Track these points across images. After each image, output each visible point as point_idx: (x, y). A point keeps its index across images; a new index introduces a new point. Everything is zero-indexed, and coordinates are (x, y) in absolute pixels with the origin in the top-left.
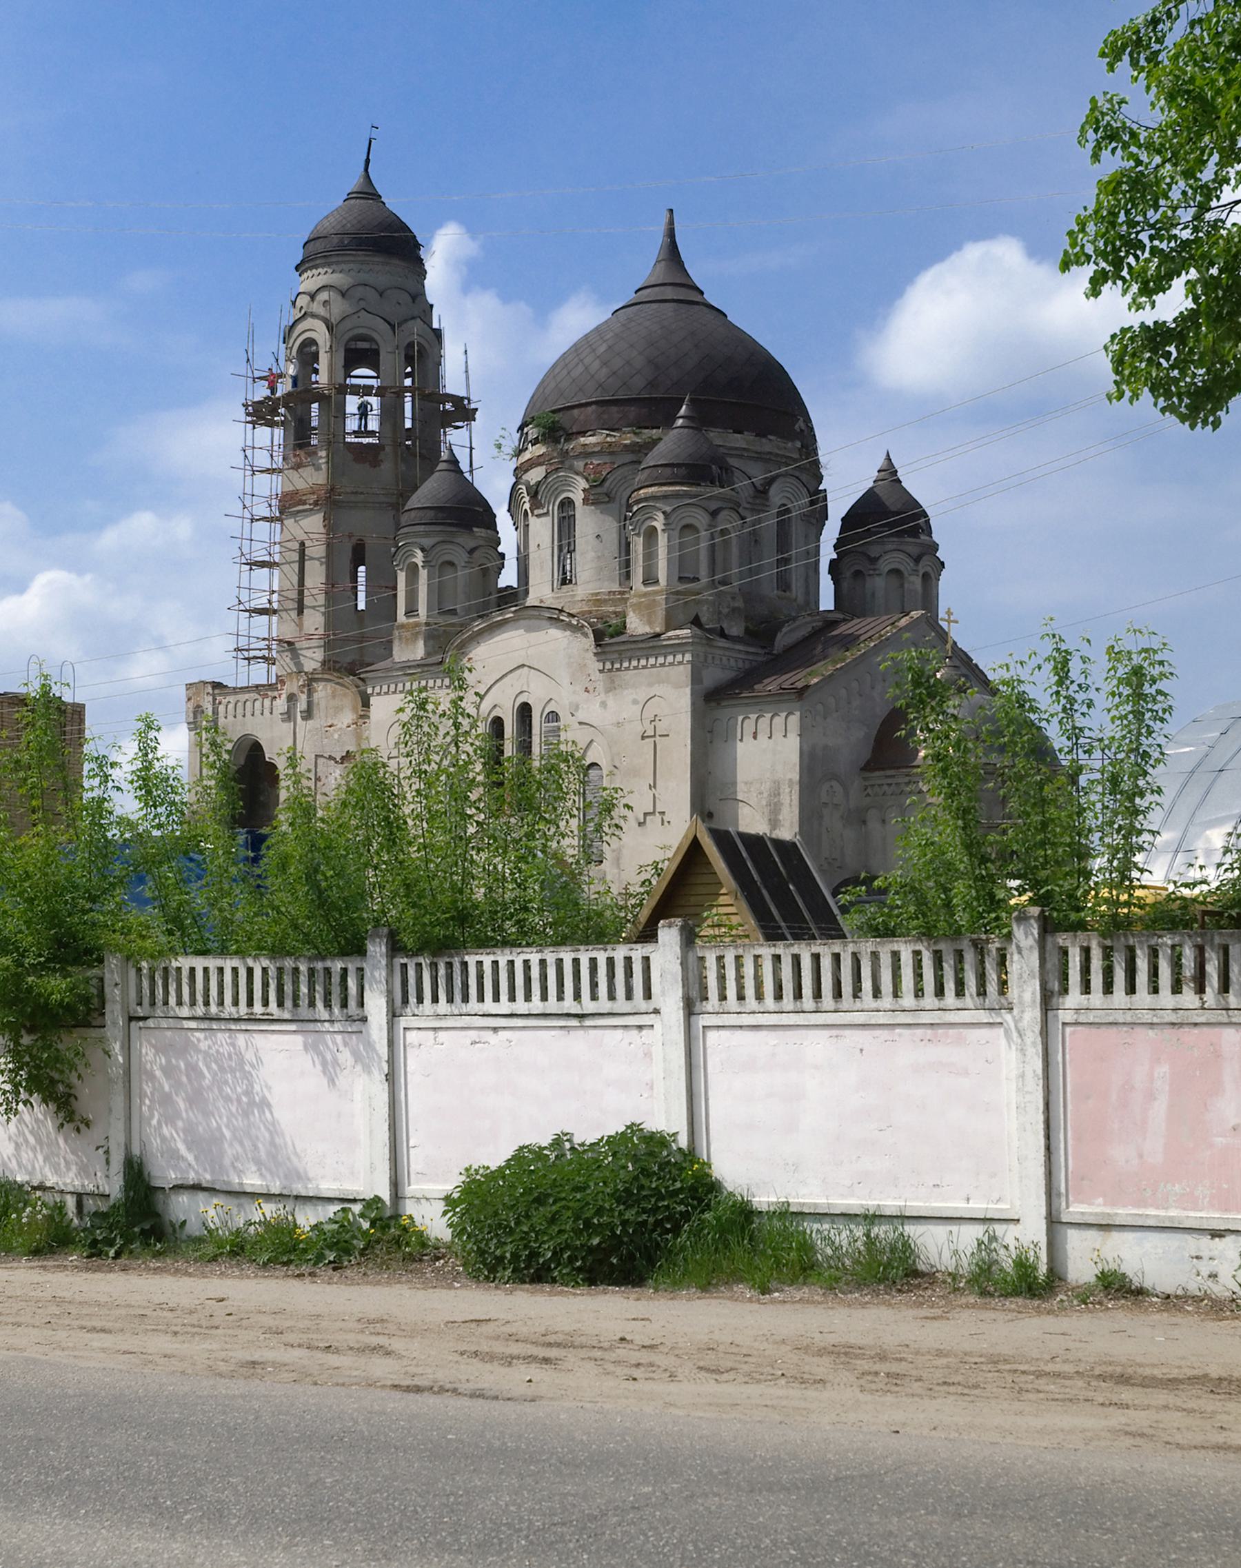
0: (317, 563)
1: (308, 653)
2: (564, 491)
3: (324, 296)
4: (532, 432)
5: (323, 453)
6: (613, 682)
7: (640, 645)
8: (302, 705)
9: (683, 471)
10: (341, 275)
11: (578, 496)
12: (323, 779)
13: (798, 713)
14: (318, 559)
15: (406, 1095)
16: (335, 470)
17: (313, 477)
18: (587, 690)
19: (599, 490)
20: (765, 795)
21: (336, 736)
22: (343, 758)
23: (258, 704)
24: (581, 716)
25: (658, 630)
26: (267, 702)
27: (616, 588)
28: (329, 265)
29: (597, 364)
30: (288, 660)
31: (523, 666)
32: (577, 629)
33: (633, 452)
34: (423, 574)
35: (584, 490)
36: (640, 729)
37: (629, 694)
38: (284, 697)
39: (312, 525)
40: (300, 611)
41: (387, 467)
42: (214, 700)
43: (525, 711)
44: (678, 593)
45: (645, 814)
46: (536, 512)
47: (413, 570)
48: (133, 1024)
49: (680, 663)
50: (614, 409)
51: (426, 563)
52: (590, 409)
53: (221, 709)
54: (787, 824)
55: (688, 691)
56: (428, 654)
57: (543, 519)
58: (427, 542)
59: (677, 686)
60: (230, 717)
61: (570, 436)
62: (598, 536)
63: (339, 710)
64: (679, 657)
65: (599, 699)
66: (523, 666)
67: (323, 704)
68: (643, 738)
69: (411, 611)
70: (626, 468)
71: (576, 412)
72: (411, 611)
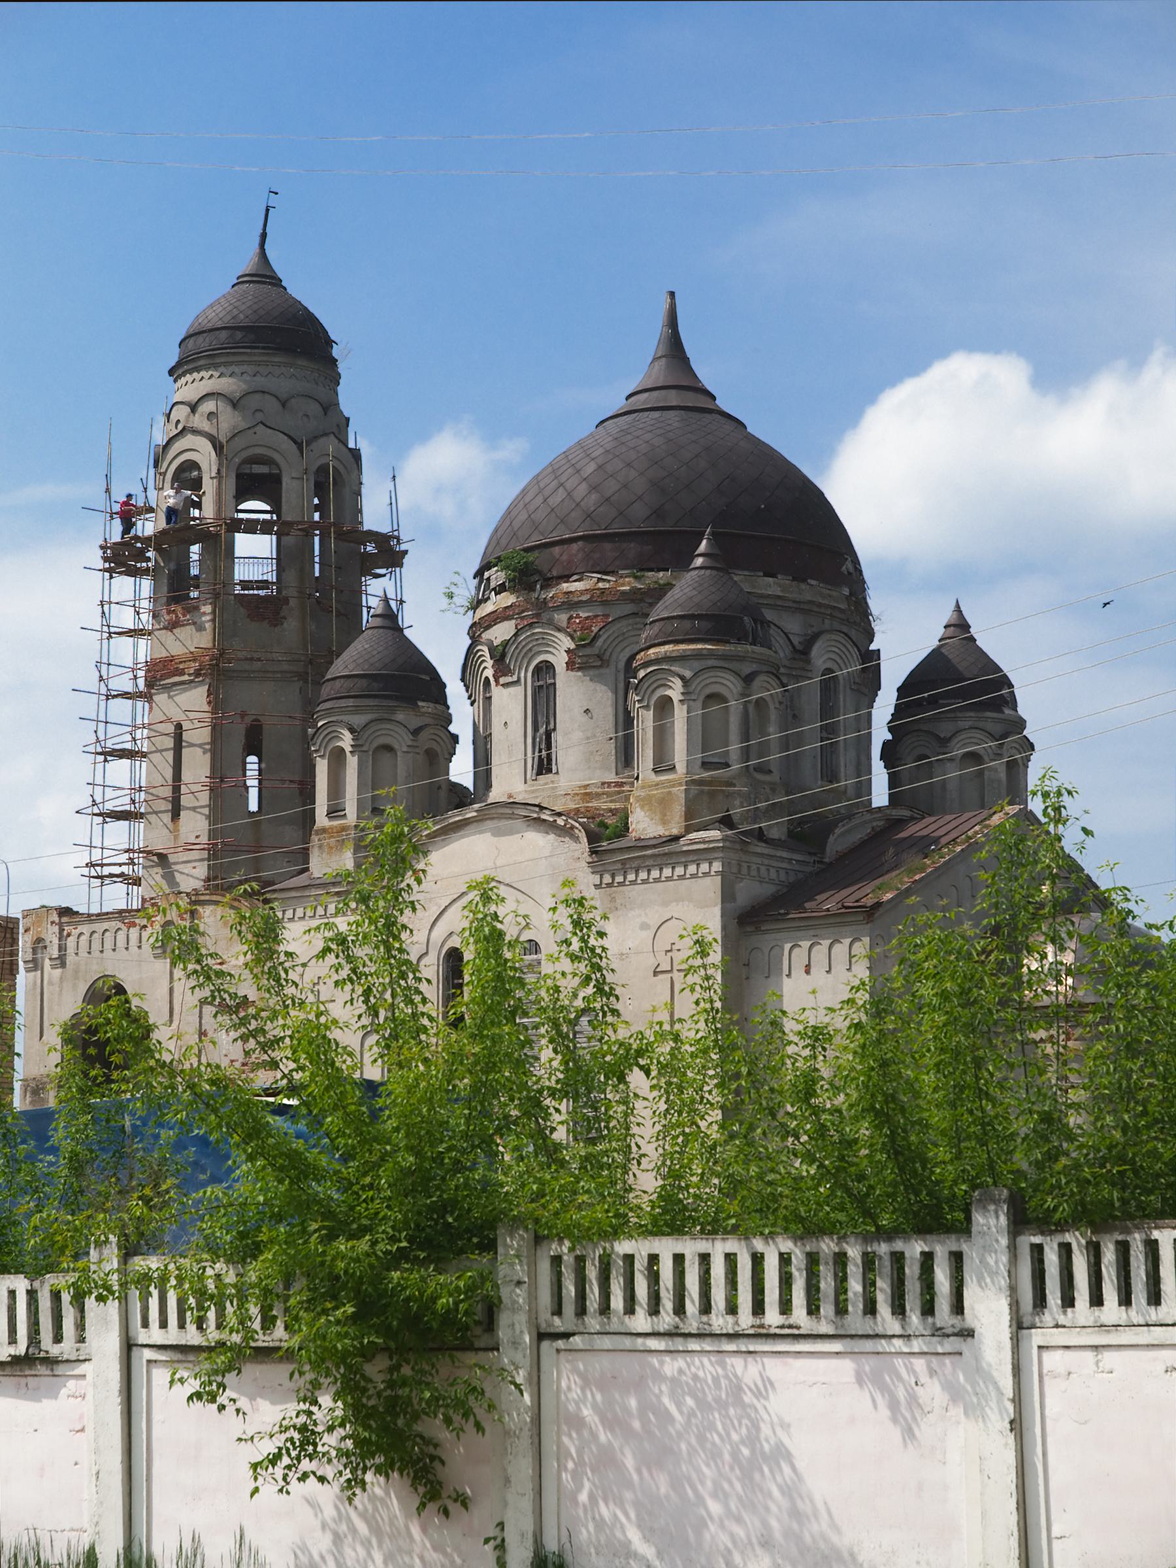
0: (199, 751)
1: (187, 868)
2: (540, 652)
3: (209, 406)
4: (497, 576)
5: (208, 609)
6: (613, 900)
9: (706, 625)
10: (230, 380)
11: (559, 659)
13: (866, 940)
14: (200, 746)
15: (1044, 1454)
16: (223, 631)
17: (193, 640)
19: (588, 651)
23: (121, 936)
25: (675, 831)
26: (134, 933)
27: (612, 777)
28: (215, 366)
29: (583, 488)
30: (158, 878)
32: (566, 832)
33: (633, 601)
34: (352, 762)
35: (568, 651)
36: (651, 962)
39: (191, 703)
40: (176, 813)
41: (291, 625)
42: (61, 930)
44: (700, 782)
46: (502, 680)
47: (338, 757)
48: (545, 1344)
49: (706, 874)
50: (608, 546)
52: (575, 547)
53: (71, 942)
55: (717, 911)
57: (512, 690)
58: (358, 720)
61: (548, 583)
62: (587, 711)
64: (704, 867)
68: (656, 973)
69: (335, 811)
70: (624, 622)
71: (556, 550)
72: (335, 811)
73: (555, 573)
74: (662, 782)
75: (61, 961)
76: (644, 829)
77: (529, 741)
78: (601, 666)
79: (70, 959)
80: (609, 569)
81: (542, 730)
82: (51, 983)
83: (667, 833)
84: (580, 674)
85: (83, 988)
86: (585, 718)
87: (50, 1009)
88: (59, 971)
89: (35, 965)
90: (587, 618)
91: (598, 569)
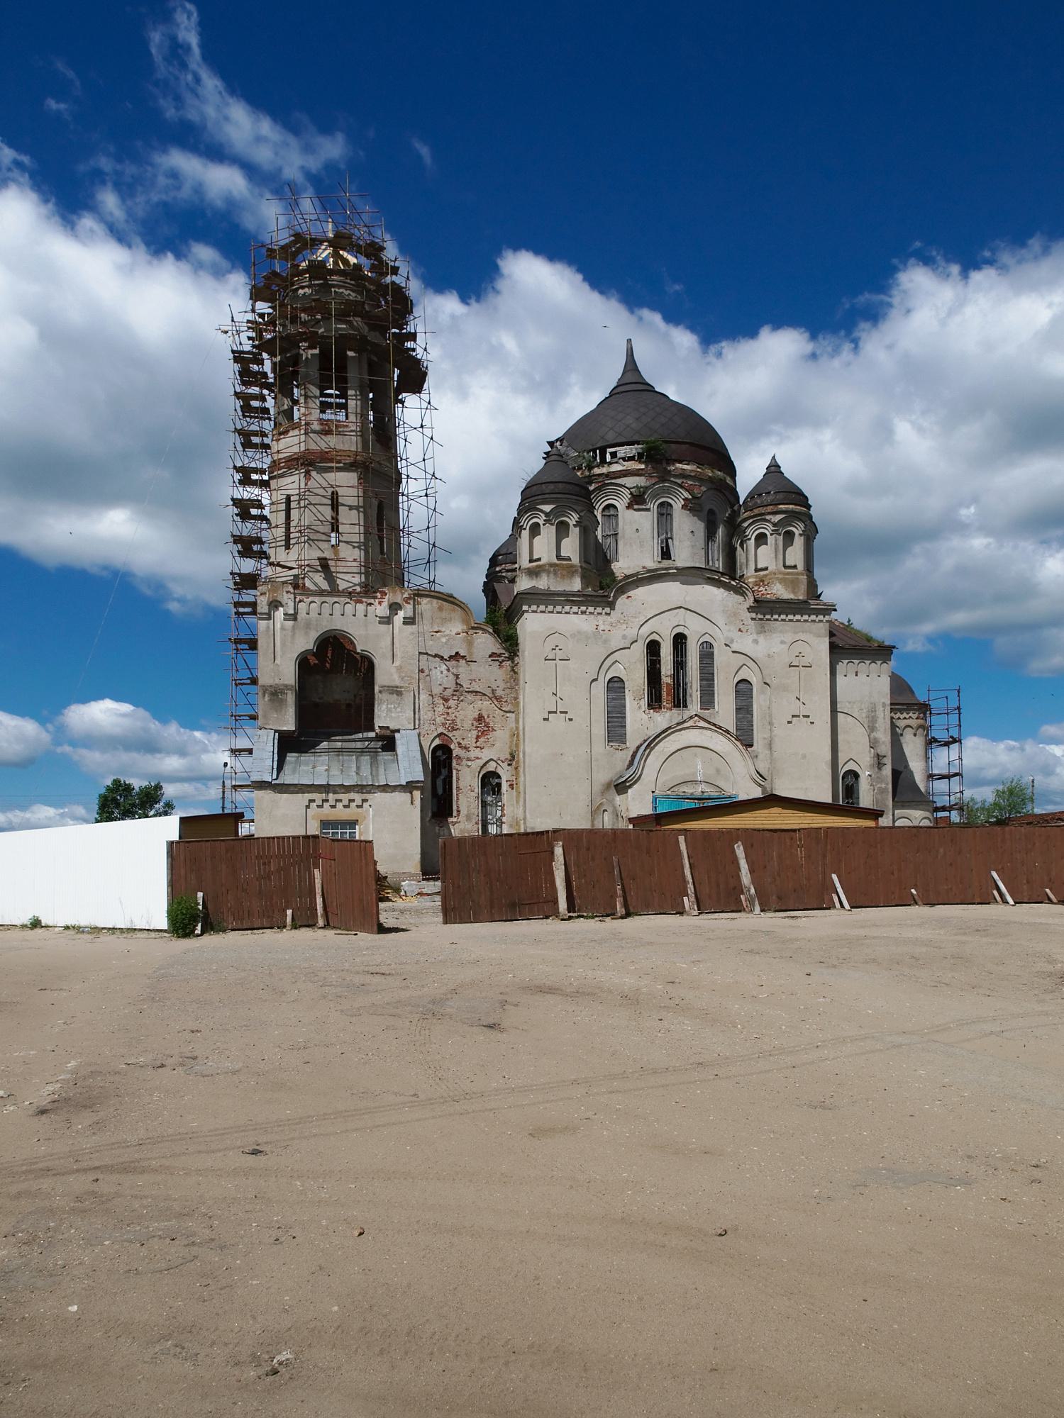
8: (407, 611)
12: (427, 672)
21: (444, 640)
22: (451, 657)
24: (735, 647)
26: (361, 607)
36: (787, 661)
38: (385, 604)
43: (680, 641)
49: (821, 621)
51: (577, 524)
52: (684, 447)
60: (314, 614)
63: (444, 621)
64: (821, 617)
65: (751, 638)
67: (427, 615)
71: (673, 446)
75: (294, 617)
79: (302, 614)
82: (283, 628)
85: (314, 635)
87: (283, 644)
88: (291, 623)
89: (269, 617)
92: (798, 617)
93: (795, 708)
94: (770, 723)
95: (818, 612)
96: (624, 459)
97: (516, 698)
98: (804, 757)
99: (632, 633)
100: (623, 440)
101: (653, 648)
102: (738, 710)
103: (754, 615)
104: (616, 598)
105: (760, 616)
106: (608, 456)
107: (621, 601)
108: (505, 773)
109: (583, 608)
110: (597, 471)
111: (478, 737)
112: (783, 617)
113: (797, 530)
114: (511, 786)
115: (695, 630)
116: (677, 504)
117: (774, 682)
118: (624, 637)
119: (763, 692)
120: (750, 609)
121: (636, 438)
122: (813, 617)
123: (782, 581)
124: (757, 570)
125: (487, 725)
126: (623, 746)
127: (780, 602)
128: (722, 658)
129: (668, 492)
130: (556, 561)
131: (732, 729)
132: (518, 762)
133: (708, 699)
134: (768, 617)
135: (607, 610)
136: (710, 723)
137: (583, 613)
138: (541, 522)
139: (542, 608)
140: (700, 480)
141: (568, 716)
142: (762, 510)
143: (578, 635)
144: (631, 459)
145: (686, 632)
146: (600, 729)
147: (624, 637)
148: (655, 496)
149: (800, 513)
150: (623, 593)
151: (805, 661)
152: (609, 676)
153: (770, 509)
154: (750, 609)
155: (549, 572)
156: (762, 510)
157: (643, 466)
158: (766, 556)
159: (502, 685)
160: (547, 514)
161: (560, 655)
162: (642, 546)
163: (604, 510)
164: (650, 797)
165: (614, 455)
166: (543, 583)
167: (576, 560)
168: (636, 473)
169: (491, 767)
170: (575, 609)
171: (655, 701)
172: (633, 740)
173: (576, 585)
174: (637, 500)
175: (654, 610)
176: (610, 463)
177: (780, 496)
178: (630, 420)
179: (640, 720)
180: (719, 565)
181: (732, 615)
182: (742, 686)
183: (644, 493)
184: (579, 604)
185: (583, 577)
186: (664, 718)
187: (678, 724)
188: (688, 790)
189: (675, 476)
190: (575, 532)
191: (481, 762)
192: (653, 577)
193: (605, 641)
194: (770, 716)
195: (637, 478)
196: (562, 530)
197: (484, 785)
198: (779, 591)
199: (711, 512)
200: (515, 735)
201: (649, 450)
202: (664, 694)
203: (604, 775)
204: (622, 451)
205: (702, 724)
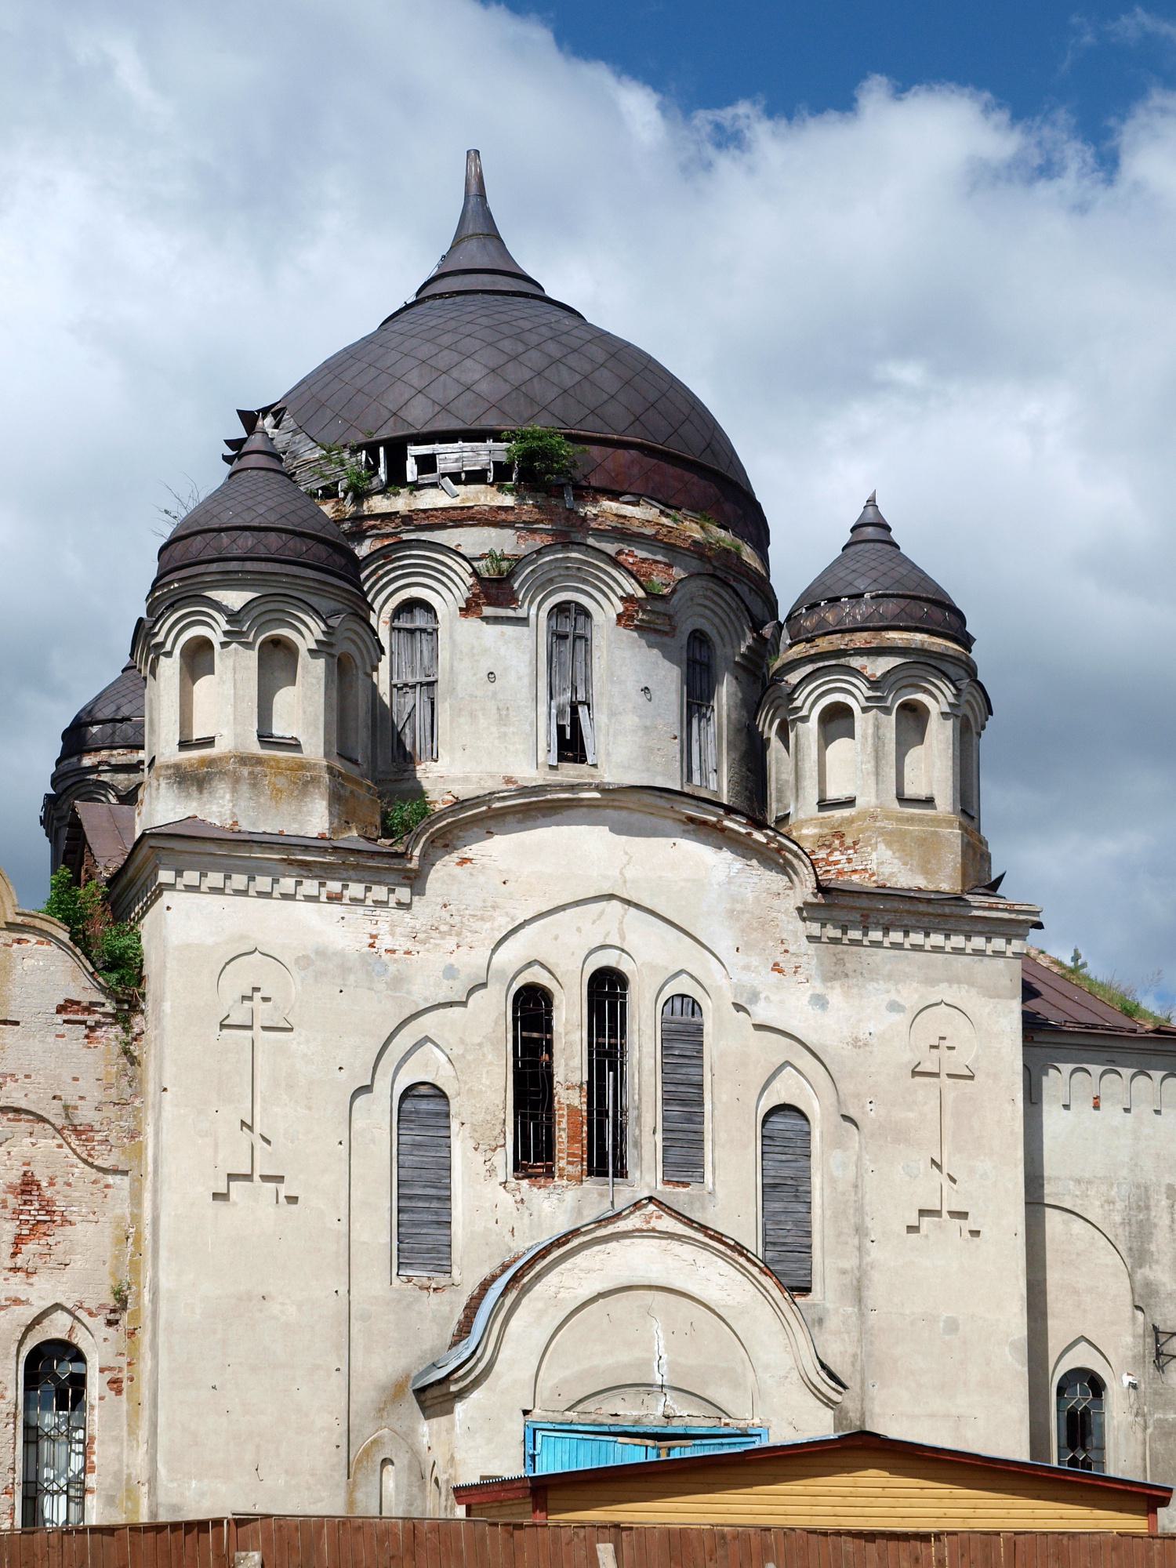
4: (481, 455)
6: (840, 962)
7: (922, 907)
18: (777, 968)
19: (660, 606)
20: (1120, 1205)
24: (763, 1013)
25: (945, 887)
31: (611, 897)
35: (628, 599)
36: (908, 1058)
37: (878, 994)
43: (607, 990)
45: (923, 1213)
46: (488, 611)
49: (999, 954)
50: (670, 470)
54: (1166, 1260)
56: (334, 830)
57: (509, 630)
59: (992, 993)
61: (587, 492)
64: (999, 943)
65: (807, 991)
66: (611, 897)
71: (594, 451)
73: (593, 483)
74: (921, 820)
76: (892, 874)
77: (543, 709)
78: (666, 633)
80: (672, 502)
81: (565, 698)
83: (931, 887)
84: (635, 634)
86: (641, 699)
90: (644, 560)
91: (660, 497)
92: (937, 939)
93: (928, 1189)
94: (860, 1230)
95: (991, 928)
96: (455, 478)
97: (134, 1134)
98: (952, 1326)
99: (471, 962)
100: (455, 425)
101: (532, 1007)
102: (770, 1189)
103: (815, 928)
104: (428, 861)
105: (832, 932)
106: (411, 467)
107: (443, 873)
108: (98, 1350)
109: (334, 886)
110: (379, 504)
111: (19, 1241)
112: (896, 936)
113: (937, 700)
114: (115, 1384)
115: (651, 965)
116: (605, 612)
117: (869, 1116)
118: (450, 972)
119: (839, 1143)
120: (806, 912)
121: (491, 422)
122: (978, 942)
123: (894, 839)
124: (824, 804)
125: (47, 1207)
126: (441, 1279)
127: (886, 895)
128: (723, 1042)
129: (578, 574)
130: (255, 748)
131: (752, 1241)
132: (136, 1316)
133: (685, 1154)
134: (855, 934)
135: (403, 894)
136: (690, 1222)
137: (334, 898)
138: (217, 638)
139: (215, 879)
140: (670, 548)
141: (284, 1190)
142: (838, 642)
143: (319, 962)
144: (476, 477)
145: (625, 966)
146: (376, 1228)
147: (450, 972)
148: (544, 584)
149: (942, 656)
150: (449, 847)
151: (954, 1063)
152: (403, 1082)
153: (860, 639)
154: (806, 912)
155: (237, 781)
156: (838, 642)
157: (509, 500)
158: (850, 766)
159: (96, 1094)
160: (233, 617)
161: (264, 1014)
162: (503, 718)
163: (397, 613)
164: (516, 1426)
165: (427, 464)
166: (218, 809)
167: (314, 749)
168: (492, 519)
169: (57, 1328)
170: (310, 886)
171: (533, 1154)
172: (470, 1264)
173: (314, 818)
174: (493, 592)
175: (539, 899)
176: (416, 487)
177: (890, 607)
178: (472, 372)
179: (491, 1205)
180: (721, 784)
181: (754, 927)
182: (779, 1122)
183: (512, 574)
184: (322, 873)
185: (336, 799)
186: (560, 1203)
187: (601, 1222)
188: (628, 1410)
189: (600, 534)
190: (312, 672)
191: (27, 1314)
192: (534, 808)
193: (397, 982)
194: (860, 1210)
195: (493, 532)
196: (277, 660)
197: (32, 1379)
198: (885, 865)
199: (698, 638)
200: (132, 1241)
201: (529, 456)
202: (561, 1136)
203: (385, 1361)
204: (450, 456)
205: (668, 1224)
